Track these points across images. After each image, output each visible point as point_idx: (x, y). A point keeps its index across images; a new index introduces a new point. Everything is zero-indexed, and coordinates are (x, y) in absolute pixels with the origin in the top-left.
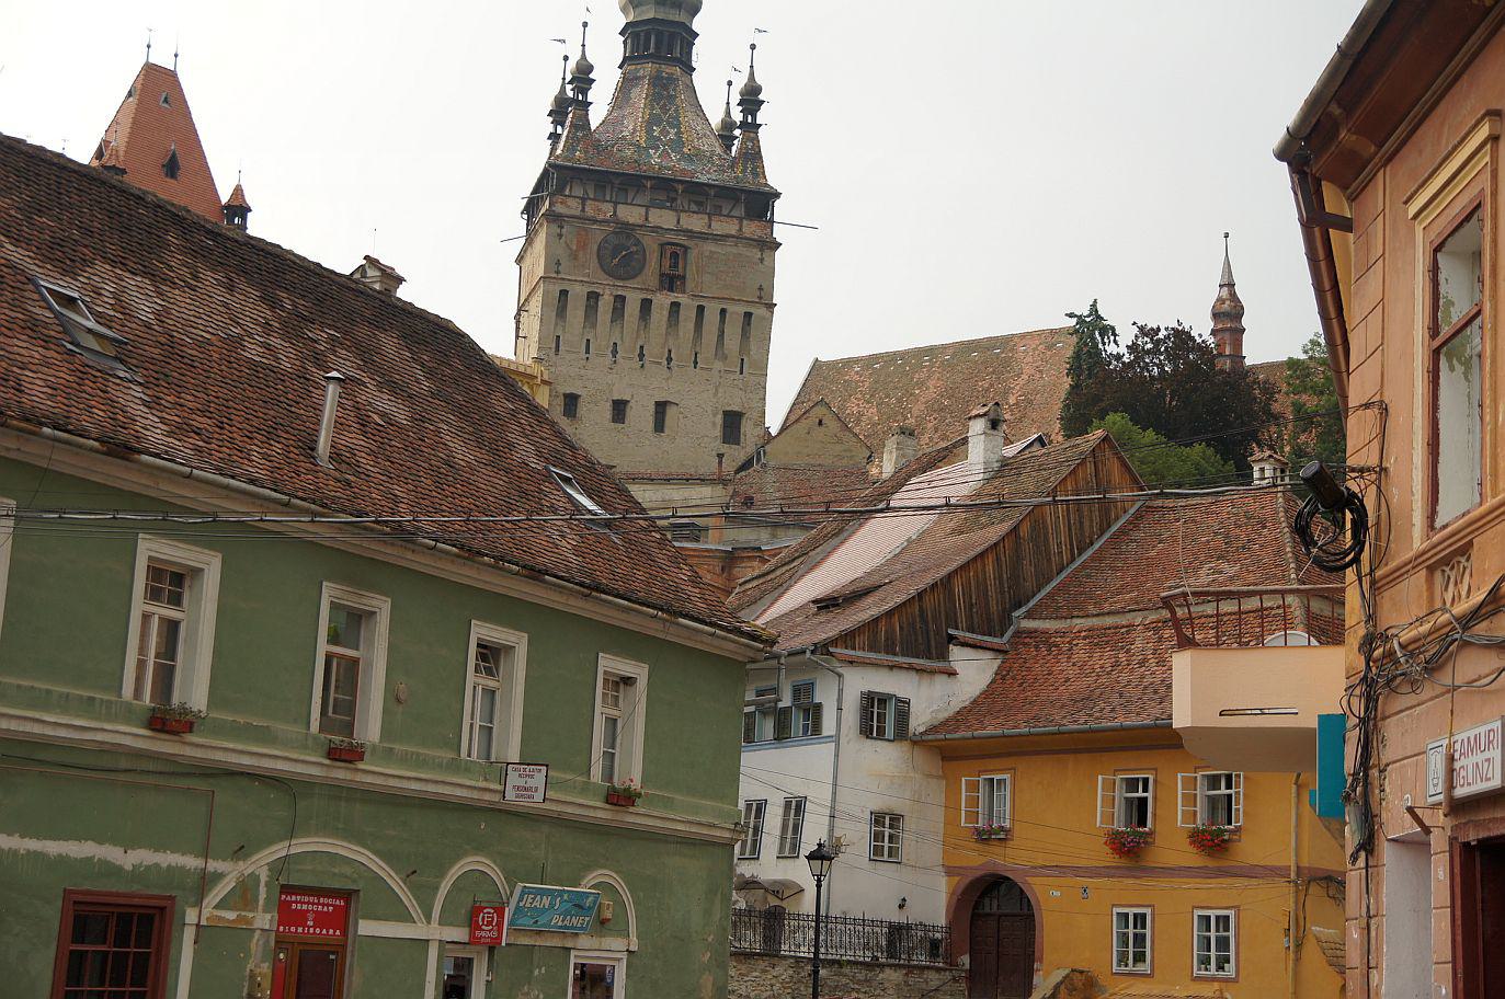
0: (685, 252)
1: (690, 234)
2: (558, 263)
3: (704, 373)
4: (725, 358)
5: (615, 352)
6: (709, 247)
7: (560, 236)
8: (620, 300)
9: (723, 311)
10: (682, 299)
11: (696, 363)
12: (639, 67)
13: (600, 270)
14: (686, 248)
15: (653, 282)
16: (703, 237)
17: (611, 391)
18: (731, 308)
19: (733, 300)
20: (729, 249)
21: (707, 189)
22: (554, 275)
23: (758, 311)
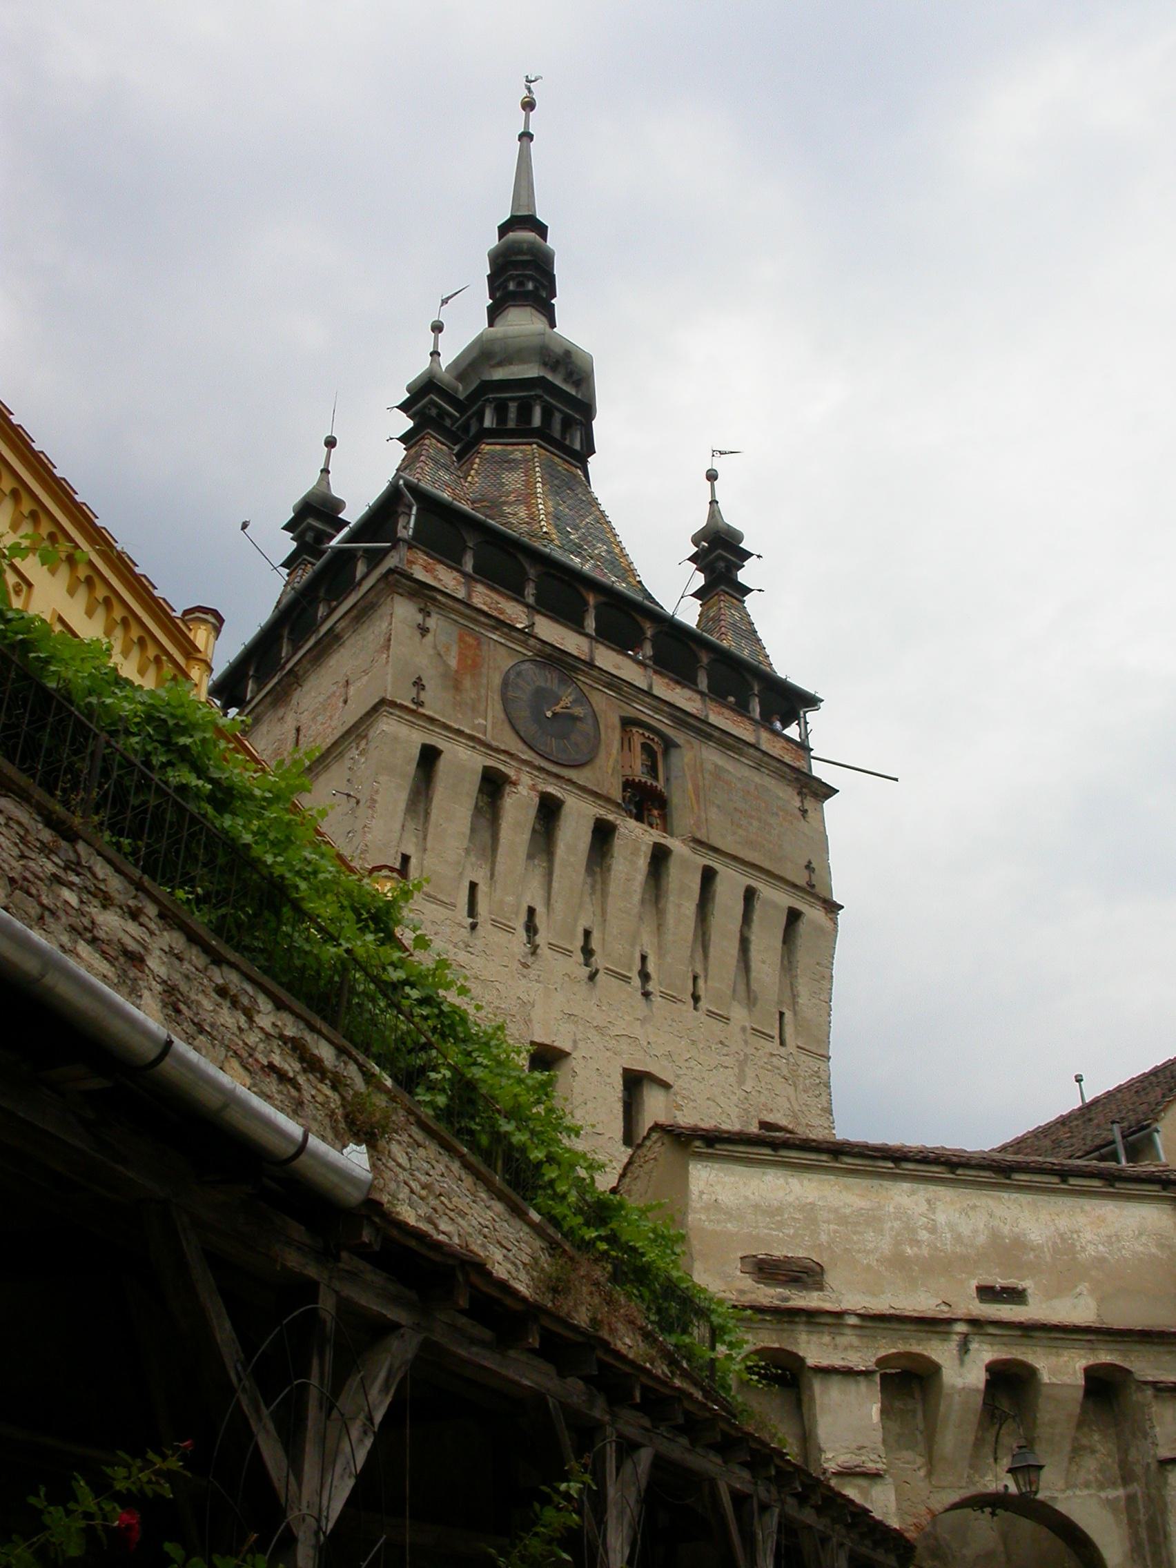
0: (666, 752)
1: (681, 718)
2: (419, 684)
3: (717, 1026)
4: (751, 1000)
5: (531, 928)
6: (712, 756)
7: (424, 631)
8: (549, 810)
9: (750, 895)
10: (674, 844)
11: (696, 998)
12: (510, 448)
13: (507, 727)
14: (669, 745)
15: (617, 794)
17: (528, 1022)
20: (747, 772)
21: (694, 646)
22: (413, 707)
23: (813, 914)
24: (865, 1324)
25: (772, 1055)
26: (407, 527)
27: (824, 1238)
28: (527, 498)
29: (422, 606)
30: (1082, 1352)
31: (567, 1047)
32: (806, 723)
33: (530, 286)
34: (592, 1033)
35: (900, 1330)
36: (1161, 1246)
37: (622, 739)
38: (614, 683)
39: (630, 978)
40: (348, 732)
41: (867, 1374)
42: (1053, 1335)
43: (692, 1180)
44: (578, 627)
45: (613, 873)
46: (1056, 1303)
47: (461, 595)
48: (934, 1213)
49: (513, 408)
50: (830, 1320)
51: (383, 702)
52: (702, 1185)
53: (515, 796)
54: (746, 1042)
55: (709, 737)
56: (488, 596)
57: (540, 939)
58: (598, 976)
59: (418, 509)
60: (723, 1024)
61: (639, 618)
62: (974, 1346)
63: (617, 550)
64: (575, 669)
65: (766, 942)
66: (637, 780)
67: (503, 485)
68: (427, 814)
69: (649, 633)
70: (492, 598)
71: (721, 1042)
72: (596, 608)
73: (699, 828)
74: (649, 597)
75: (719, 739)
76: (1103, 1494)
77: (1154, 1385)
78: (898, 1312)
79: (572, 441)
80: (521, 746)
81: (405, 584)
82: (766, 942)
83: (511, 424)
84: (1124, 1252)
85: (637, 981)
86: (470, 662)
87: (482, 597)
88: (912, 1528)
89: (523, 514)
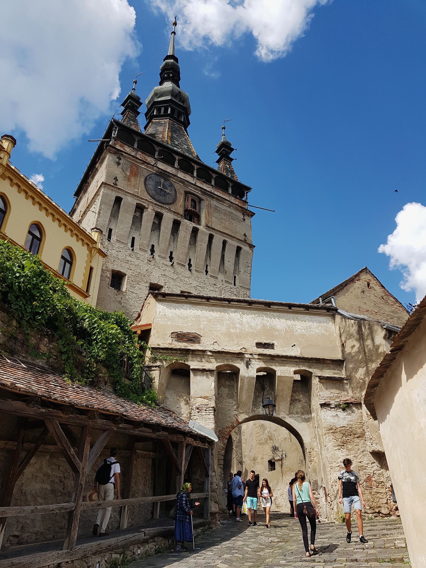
0: (200, 202)
1: (204, 192)
2: (116, 179)
5: (152, 251)
6: (214, 203)
8: (159, 216)
10: (201, 228)
11: (207, 272)
12: (161, 120)
13: (145, 192)
14: (200, 200)
16: (212, 196)
18: (229, 241)
19: (231, 236)
20: (225, 208)
22: (113, 185)
23: (245, 248)
24: (213, 354)
25: (231, 288)
26: (114, 134)
27: (202, 326)
28: (163, 133)
29: (118, 156)
30: (293, 365)
31: (162, 284)
32: (247, 195)
33: (171, 75)
34: (171, 280)
35: (225, 357)
36: (326, 331)
37: (185, 198)
38: (182, 181)
39: (185, 265)
40: (95, 195)
41: (211, 371)
42: (282, 359)
43: (158, 308)
44: (172, 165)
45: (179, 235)
46: (284, 349)
47: (133, 154)
48: (242, 319)
49: (163, 109)
50: (200, 353)
51: (103, 182)
52: (161, 310)
53: (147, 212)
54: (223, 284)
55: (214, 198)
56: (141, 155)
57: (154, 254)
58: (174, 264)
59: (118, 129)
60: (215, 279)
61: (192, 164)
62: (253, 361)
63: (190, 147)
64: (169, 177)
65: (230, 256)
66: (189, 209)
67: (157, 130)
68: (118, 217)
69: (196, 168)
70: (143, 156)
71: (214, 284)
72: (178, 160)
73: (208, 223)
74: (200, 160)
75: (216, 198)
76: (303, 416)
77: (319, 377)
78: (226, 351)
79: (181, 119)
80: (150, 197)
81: (112, 150)
82: (230, 256)
83: (162, 113)
84: (312, 332)
85: (187, 267)
86: (134, 173)
87: (139, 155)
88: (230, 427)
89: (161, 136)
